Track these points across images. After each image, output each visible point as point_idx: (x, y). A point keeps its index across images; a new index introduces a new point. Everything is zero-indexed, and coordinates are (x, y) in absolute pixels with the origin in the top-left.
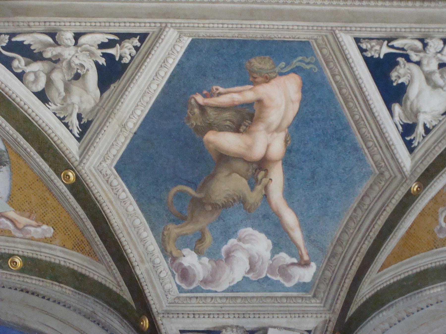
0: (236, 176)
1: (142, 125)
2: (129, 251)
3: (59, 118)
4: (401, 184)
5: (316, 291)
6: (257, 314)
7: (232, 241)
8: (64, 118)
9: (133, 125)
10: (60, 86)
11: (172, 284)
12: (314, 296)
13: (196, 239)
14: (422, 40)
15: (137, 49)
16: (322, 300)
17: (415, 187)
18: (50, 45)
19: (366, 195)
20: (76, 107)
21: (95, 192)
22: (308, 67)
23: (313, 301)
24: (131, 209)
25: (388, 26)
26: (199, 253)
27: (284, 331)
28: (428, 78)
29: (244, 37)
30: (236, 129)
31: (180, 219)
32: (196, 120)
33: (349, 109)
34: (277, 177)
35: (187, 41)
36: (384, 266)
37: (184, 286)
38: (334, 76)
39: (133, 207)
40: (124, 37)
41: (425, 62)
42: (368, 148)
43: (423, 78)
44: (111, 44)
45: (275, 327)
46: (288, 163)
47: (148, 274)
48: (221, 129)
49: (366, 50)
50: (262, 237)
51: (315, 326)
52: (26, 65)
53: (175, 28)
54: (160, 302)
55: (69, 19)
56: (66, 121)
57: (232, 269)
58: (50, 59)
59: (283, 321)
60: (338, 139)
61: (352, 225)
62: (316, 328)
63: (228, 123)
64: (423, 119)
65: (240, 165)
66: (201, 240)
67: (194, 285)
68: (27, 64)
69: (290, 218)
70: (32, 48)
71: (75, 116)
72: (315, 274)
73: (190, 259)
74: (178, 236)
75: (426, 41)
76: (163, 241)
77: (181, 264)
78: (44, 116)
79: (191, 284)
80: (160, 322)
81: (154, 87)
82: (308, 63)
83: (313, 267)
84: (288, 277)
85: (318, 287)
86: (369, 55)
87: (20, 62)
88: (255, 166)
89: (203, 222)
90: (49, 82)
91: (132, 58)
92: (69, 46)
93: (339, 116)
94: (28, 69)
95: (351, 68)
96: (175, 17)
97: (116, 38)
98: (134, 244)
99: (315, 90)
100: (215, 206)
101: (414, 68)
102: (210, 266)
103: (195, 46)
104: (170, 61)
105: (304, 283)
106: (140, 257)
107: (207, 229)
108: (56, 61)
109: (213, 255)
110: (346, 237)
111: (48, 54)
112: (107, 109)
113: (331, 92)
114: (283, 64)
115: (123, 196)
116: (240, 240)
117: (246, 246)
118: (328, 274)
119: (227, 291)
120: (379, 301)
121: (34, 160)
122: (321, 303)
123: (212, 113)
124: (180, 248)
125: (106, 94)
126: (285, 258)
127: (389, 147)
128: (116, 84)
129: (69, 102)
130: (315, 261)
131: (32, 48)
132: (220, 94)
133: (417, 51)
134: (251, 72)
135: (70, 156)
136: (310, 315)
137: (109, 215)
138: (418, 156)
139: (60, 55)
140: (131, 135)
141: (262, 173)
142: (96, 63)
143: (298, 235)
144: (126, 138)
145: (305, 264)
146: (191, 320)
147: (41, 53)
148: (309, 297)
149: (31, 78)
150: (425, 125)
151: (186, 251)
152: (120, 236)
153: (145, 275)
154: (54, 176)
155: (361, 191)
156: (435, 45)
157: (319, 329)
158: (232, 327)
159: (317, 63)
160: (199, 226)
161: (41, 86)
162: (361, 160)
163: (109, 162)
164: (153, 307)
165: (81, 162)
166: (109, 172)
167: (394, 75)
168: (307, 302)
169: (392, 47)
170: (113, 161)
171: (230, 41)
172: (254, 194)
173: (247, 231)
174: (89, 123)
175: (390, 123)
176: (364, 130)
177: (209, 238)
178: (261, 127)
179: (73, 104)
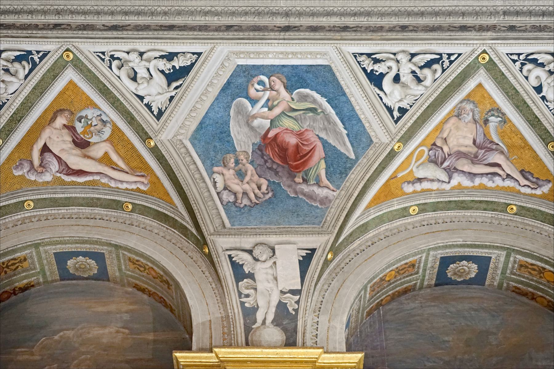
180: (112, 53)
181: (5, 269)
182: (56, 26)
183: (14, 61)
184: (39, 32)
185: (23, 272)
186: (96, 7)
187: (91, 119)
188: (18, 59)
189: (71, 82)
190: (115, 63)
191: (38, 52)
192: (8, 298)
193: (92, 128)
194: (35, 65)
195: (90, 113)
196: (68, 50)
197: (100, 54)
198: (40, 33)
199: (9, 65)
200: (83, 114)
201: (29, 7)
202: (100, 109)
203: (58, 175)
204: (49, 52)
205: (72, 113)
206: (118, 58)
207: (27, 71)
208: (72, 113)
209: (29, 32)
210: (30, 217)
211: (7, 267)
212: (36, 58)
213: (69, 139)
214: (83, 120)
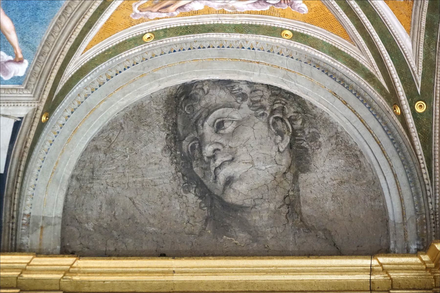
5: (27, 83)
12: (26, 88)
16: (32, 91)
36: (86, 49)
51: (26, 113)
62: (27, 116)
72: (27, 69)
85: (29, 80)
105: (19, 77)
110: (52, 39)
118: (38, 69)
120: (82, 72)
122: (31, 94)
130: (28, 58)
136: (22, 104)
148: (22, 89)
168: (21, 93)
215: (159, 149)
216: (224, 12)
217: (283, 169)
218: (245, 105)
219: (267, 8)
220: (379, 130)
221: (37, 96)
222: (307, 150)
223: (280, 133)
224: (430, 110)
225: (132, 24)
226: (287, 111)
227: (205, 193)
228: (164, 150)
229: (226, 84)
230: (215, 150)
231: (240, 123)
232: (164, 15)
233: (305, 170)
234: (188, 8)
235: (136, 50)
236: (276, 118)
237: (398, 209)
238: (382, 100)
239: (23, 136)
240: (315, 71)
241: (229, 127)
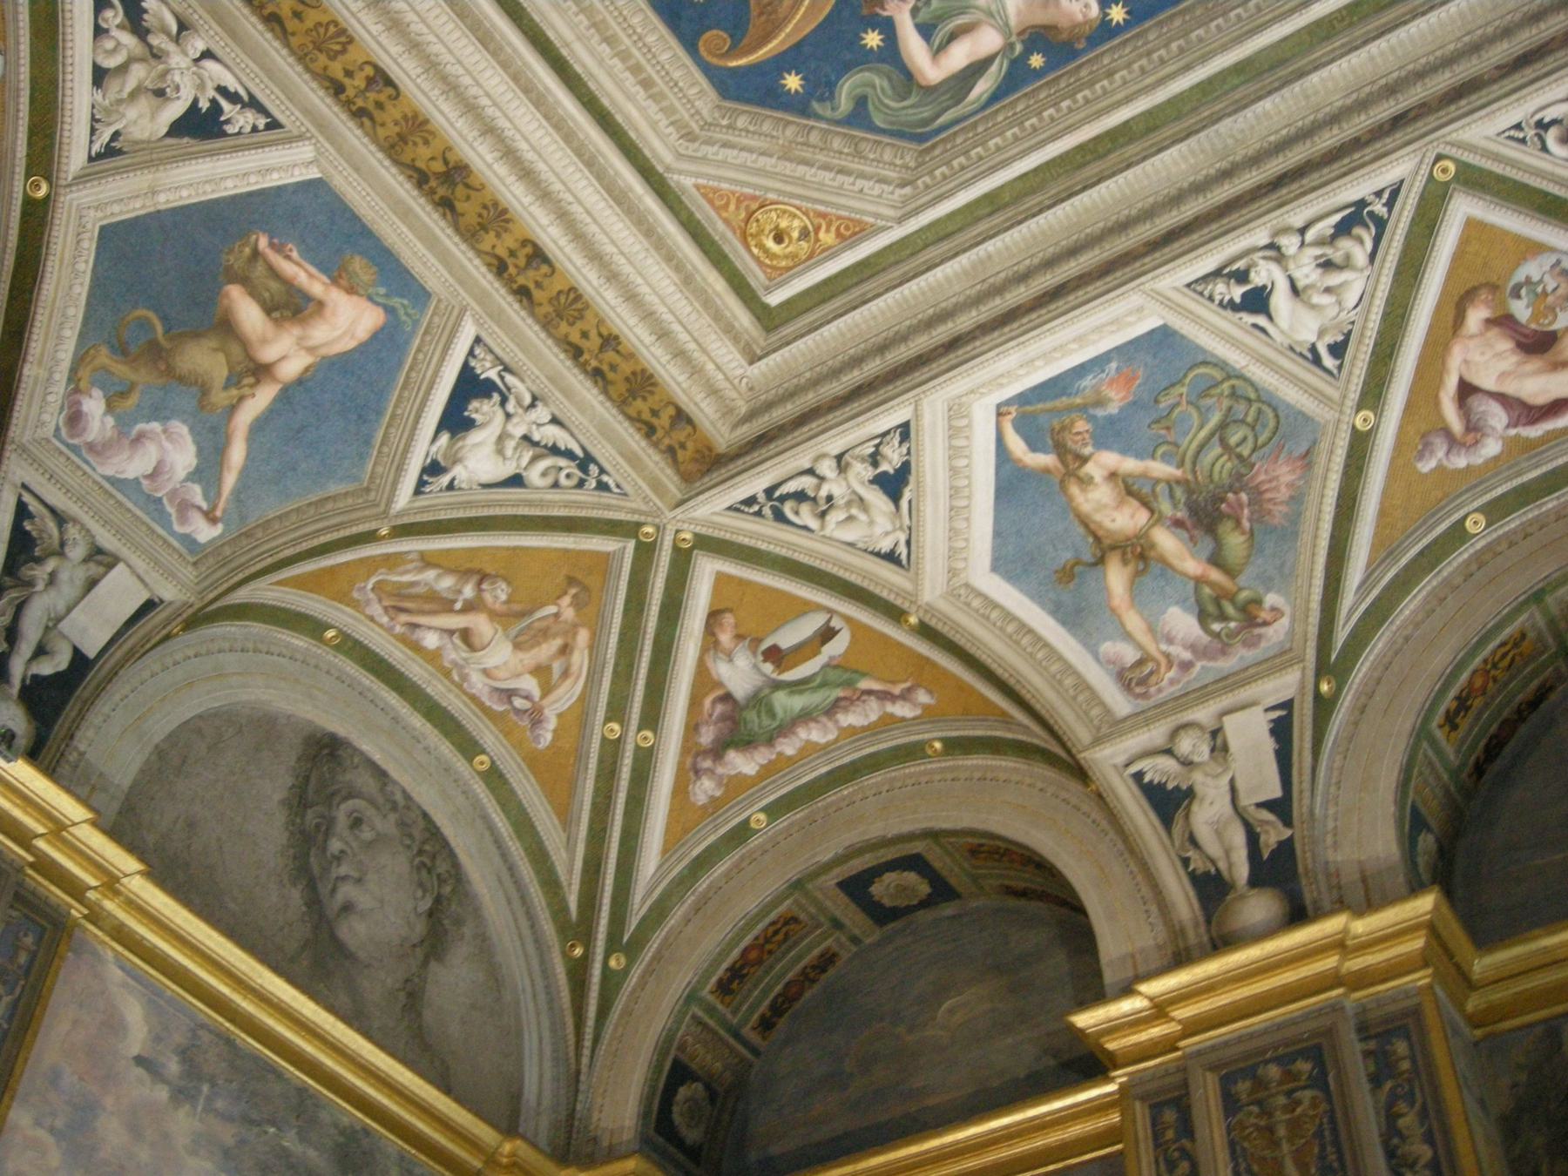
0: (221, 357)
1: (175, 211)
2: (35, 337)
3: (93, 115)
4: (376, 517)
6: (119, 532)
7: (156, 426)
8: (98, 121)
9: (165, 201)
10: (131, 83)
11: (53, 418)
12: (195, 564)
13: (119, 389)
14: (535, 398)
15: (255, 129)
17: (384, 532)
18: (168, 33)
19: (334, 498)
20: (124, 122)
21: (54, 233)
22: (404, 318)
23: (190, 568)
24: (77, 289)
25: (520, 355)
26: (110, 408)
27: (135, 579)
28: (502, 438)
29: (374, 228)
30: (269, 309)
31: (121, 351)
32: (237, 258)
33: (400, 396)
34: (262, 398)
35: (313, 173)
36: (279, 583)
37: (64, 432)
38: (419, 350)
39: (82, 290)
40: (254, 104)
41: (515, 420)
42: (379, 452)
43: (498, 433)
44: (233, 98)
45: (129, 566)
46: (287, 394)
47: (35, 383)
48: (254, 293)
49: (474, 357)
50: (192, 449)
52: (118, 26)
53: (317, 150)
54: (24, 427)
55: (219, 30)
56: (97, 126)
57: (130, 458)
58: (150, 47)
59: (141, 565)
60: (360, 416)
61: (294, 518)
62: (171, 603)
63: (267, 295)
64: (459, 472)
65: (236, 350)
66: (123, 395)
67: (75, 441)
68: (120, 27)
69: (237, 454)
70: (146, 16)
71: (112, 130)
73: (94, 405)
74: (104, 368)
75: (540, 404)
76: (82, 359)
77: (79, 403)
78: (79, 97)
79: (72, 436)
80: (7, 454)
81: (229, 183)
82: (407, 314)
83: (218, 530)
84: (183, 519)
85: (206, 556)
86: (473, 363)
87: (115, 16)
88: (251, 365)
89: (143, 376)
90: (123, 69)
91: (239, 133)
92: (185, 54)
93: (382, 395)
94: (115, 33)
95: (442, 359)
96: (328, 139)
97: (246, 98)
98: (47, 334)
99: (385, 349)
100: (170, 371)
101: (500, 416)
102: (109, 434)
103: (316, 188)
104: (275, 176)
106: (42, 355)
107: (140, 387)
108: (156, 55)
109: (123, 424)
111: (154, 40)
112: (154, 156)
113: (400, 364)
114: (382, 291)
115: (81, 266)
116: (165, 431)
117: (167, 445)
118: (227, 551)
119: (107, 478)
121: (16, 132)
123: (260, 269)
124: (93, 384)
125: (170, 141)
126: (196, 494)
127: (400, 469)
128: (192, 141)
129: (121, 109)
130: (227, 525)
131: (146, 16)
132: (288, 258)
133: (519, 402)
134: (343, 268)
135: (64, 168)
137: (48, 275)
138: (417, 504)
139: (167, 54)
140: (152, 209)
141: (251, 380)
142: (196, 101)
143: (230, 480)
144: (143, 207)
145: (211, 518)
146: (43, 480)
147: (148, 31)
149: (109, 45)
150: (453, 479)
151: (97, 393)
152: (40, 311)
153: (31, 381)
154: (20, 169)
155: (334, 488)
156: (542, 413)
157: (174, 606)
158: (83, 527)
159: (416, 323)
160: (133, 377)
161: (110, 63)
162: (362, 457)
163: (100, 214)
164: (13, 428)
165: (69, 185)
166: (89, 226)
167: (475, 404)
169: (502, 378)
170: (105, 217)
171: (355, 218)
172: (224, 394)
173: (183, 429)
174: (120, 152)
175: (425, 444)
176: (393, 430)
177: (133, 400)
178: (296, 331)
179: (123, 116)
180: (1537, 117)
181: (1493, 672)
182: (1398, 121)
183: (1334, 237)
184: (1367, 151)
185: (1526, 665)
186: (1467, 39)
187: (1541, 281)
188: (1343, 229)
189: (1473, 227)
190: (1551, 137)
191: (1379, 194)
192: (1514, 730)
193: (1550, 299)
194: (1381, 224)
195: (1533, 269)
196: (1439, 158)
197: (1512, 133)
198: (1369, 153)
199: (1329, 251)
200: (1520, 276)
201: (1328, 109)
202: (1552, 250)
203: (1513, 432)
204: (1402, 182)
205: (1494, 288)
206: (1554, 122)
207: (1369, 245)
208: (1494, 288)
209: (1346, 161)
210: (1488, 547)
211: (1495, 666)
212: (1379, 208)
213: (1505, 345)
214: (1523, 292)
215: (277, 797)
216: (447, 674)
217: (415, 938)
218: (393, 817)
219: (499, 708)
220: (535, 963)
221: (199, 588)
222: (446, 932)
223: (421, 885)
224: (626, 972)
225: (343, 598)
226: (438, 862)
227: (314, 902)
228: (283, 802)
229: (381, 774)
230: (342, 852)
231: (380, 839)
232: (385, 620)
233: (440, 958)
234: (419, 634)
235: (300, 642)
236: (423, 864)
237: (534, 1089)
238: (548, 928)
239: (149, 626)
240: (487, 834)
241: (367, 835)
